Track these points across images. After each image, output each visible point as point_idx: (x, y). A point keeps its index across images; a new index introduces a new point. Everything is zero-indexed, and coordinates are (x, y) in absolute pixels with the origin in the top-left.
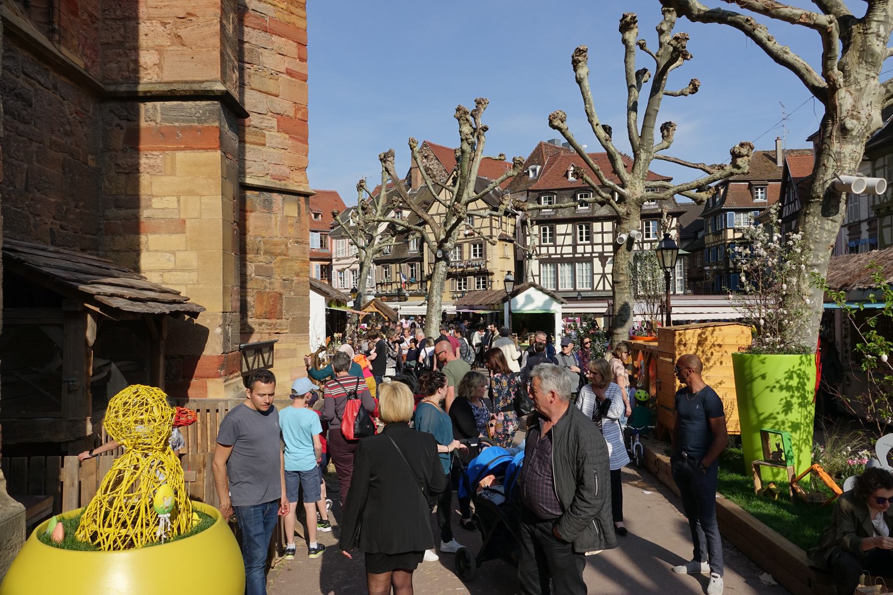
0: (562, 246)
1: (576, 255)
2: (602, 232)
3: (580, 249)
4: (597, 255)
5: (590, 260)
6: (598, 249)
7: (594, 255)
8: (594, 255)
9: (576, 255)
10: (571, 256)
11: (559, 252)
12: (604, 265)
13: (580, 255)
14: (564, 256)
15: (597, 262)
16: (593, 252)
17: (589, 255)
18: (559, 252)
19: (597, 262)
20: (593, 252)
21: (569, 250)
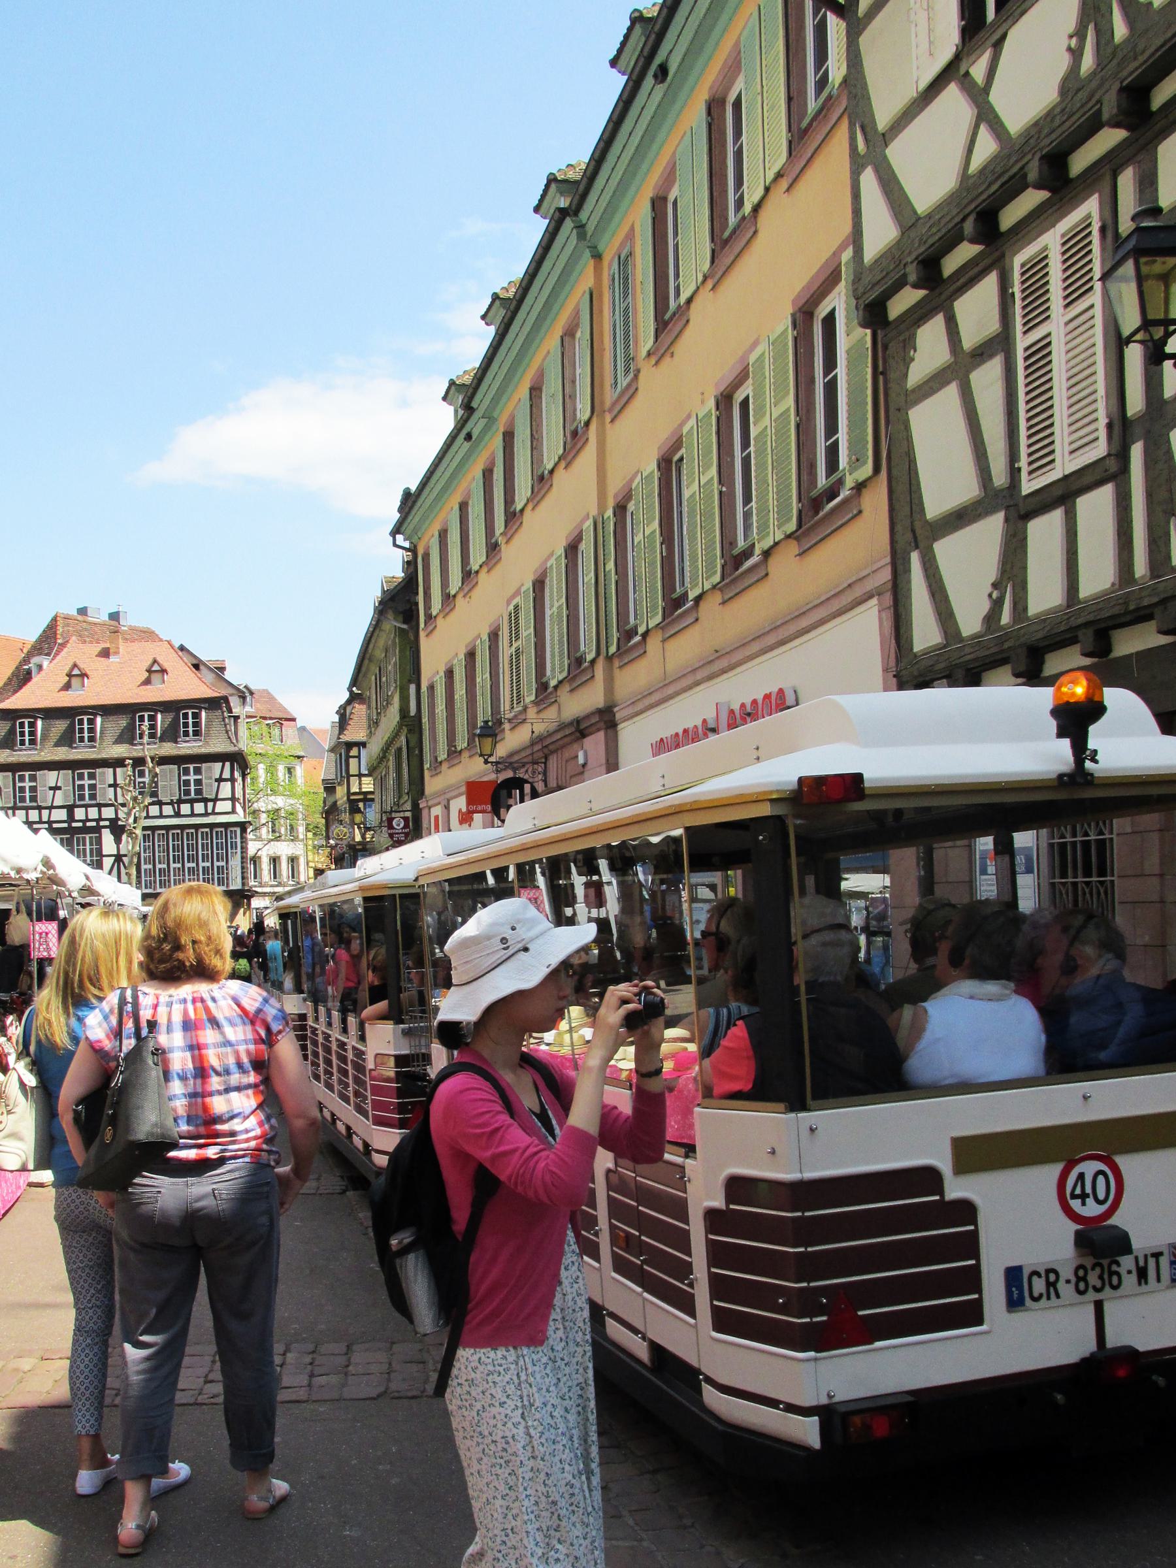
0: (51, 808)
1: (74, 825)
2: (115, 785)
3: (79, 814)
4: (107, 823)
5: (97, 830)
6: (108, 813)
7: (102, 823)
8: (102, 823)
9: (74, 825)
10: (65, 825)
11: (45, 819)
12: (118, 841)
13: (80, 824)
14: (55, 826)
15: (107, 838)
16: (100, 819)
17: (94, 824)
18: (45, 819)
19: (107, 838)
20: (100, 819)
21: (61, 815)
